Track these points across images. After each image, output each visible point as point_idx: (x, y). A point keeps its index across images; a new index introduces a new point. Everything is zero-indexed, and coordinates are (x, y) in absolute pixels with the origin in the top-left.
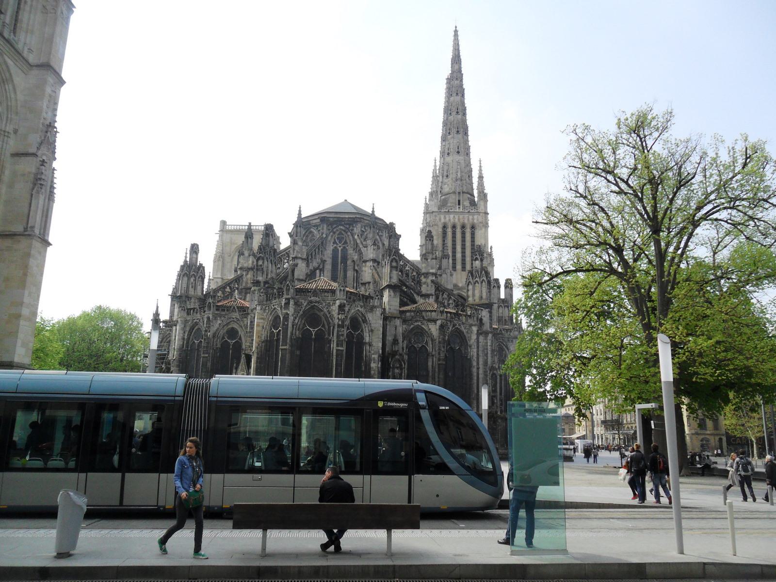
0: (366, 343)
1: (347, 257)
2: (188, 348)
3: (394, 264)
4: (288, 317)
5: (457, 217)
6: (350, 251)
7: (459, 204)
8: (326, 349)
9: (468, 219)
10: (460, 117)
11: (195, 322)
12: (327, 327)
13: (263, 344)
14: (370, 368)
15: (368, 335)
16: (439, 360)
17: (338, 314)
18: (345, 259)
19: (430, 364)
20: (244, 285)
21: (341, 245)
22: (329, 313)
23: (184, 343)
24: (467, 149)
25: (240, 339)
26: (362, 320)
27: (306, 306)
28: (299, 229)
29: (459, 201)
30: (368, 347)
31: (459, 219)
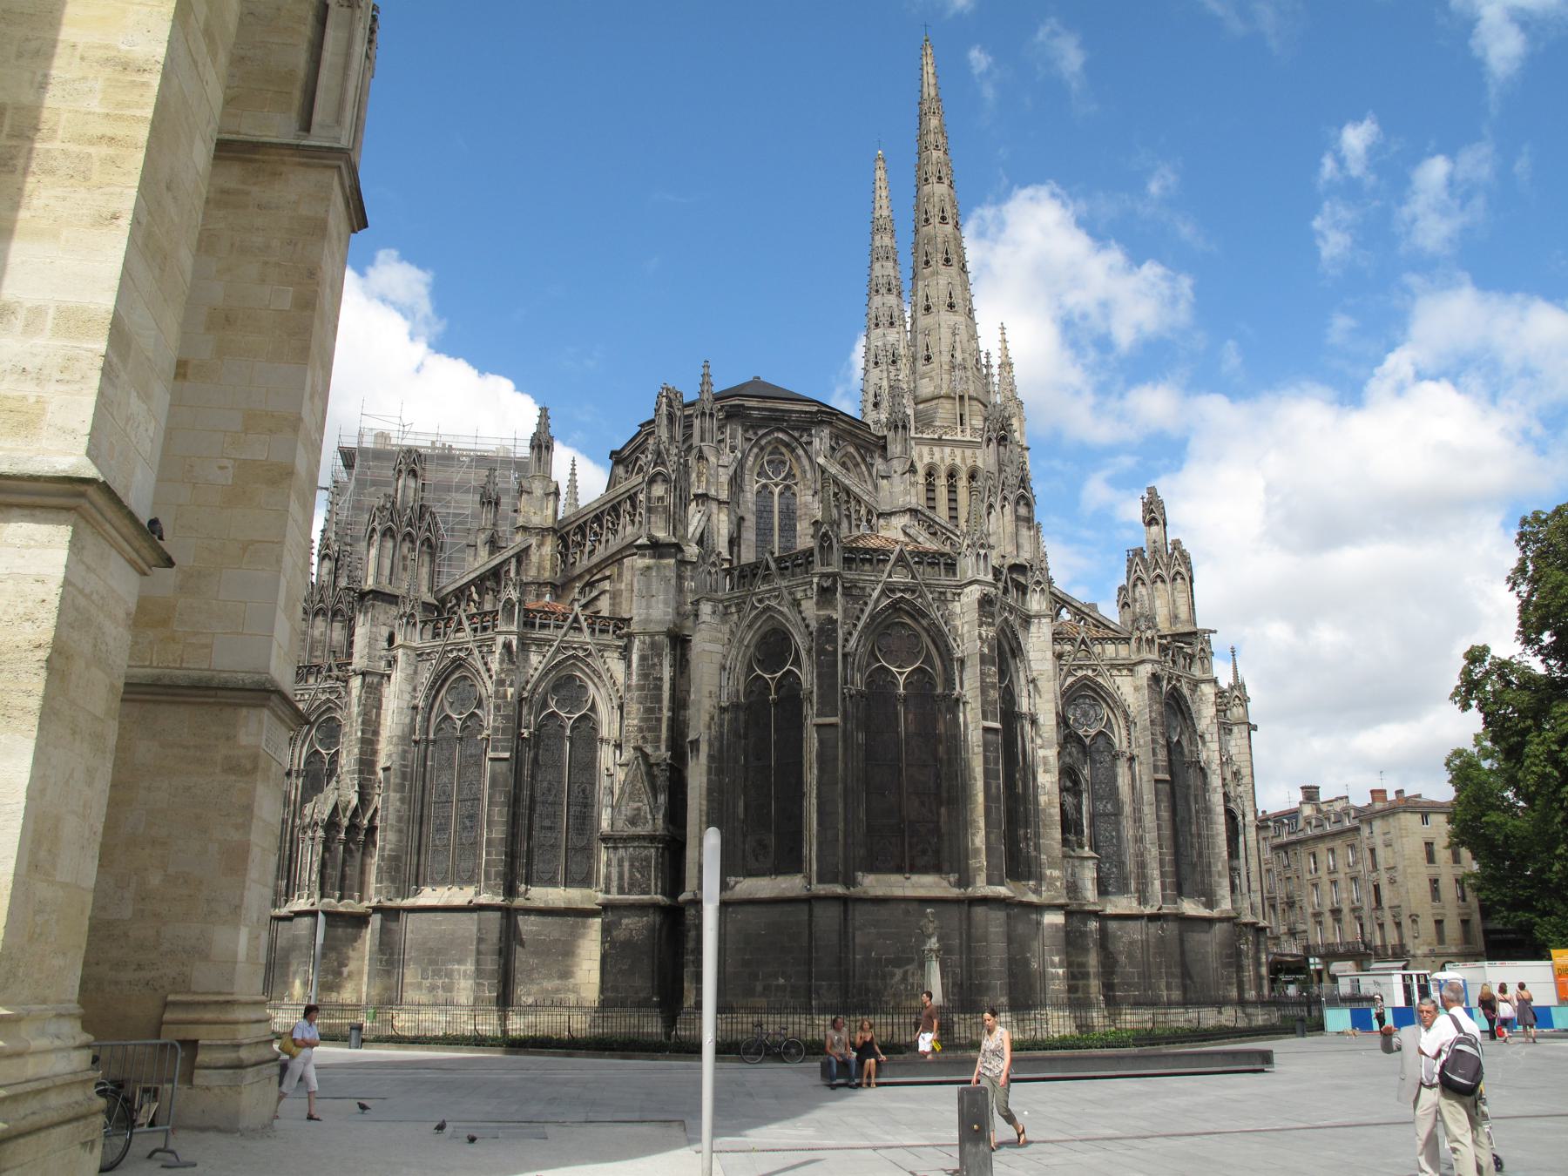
0: (1020, 716)
2: (427, 734)
3: (1023, 511)
4: (835, 631)
8: (941, 728)
10: (949, 228)
11: (454, 660)
12: (938, 662)
13: (726, 717)
14: (1036, 787)
15: (1025, 693)
16: (1156, 769)
17: (980, 626)
19: (1123, 781)
20: (533, 572)
21: (777, 480)
23: (413, 720)
25: (593, 708)
26: (1012, 650)
27: (878, 599)
29: (961, 416)
30: (1028, 727)
31: (963, 459)
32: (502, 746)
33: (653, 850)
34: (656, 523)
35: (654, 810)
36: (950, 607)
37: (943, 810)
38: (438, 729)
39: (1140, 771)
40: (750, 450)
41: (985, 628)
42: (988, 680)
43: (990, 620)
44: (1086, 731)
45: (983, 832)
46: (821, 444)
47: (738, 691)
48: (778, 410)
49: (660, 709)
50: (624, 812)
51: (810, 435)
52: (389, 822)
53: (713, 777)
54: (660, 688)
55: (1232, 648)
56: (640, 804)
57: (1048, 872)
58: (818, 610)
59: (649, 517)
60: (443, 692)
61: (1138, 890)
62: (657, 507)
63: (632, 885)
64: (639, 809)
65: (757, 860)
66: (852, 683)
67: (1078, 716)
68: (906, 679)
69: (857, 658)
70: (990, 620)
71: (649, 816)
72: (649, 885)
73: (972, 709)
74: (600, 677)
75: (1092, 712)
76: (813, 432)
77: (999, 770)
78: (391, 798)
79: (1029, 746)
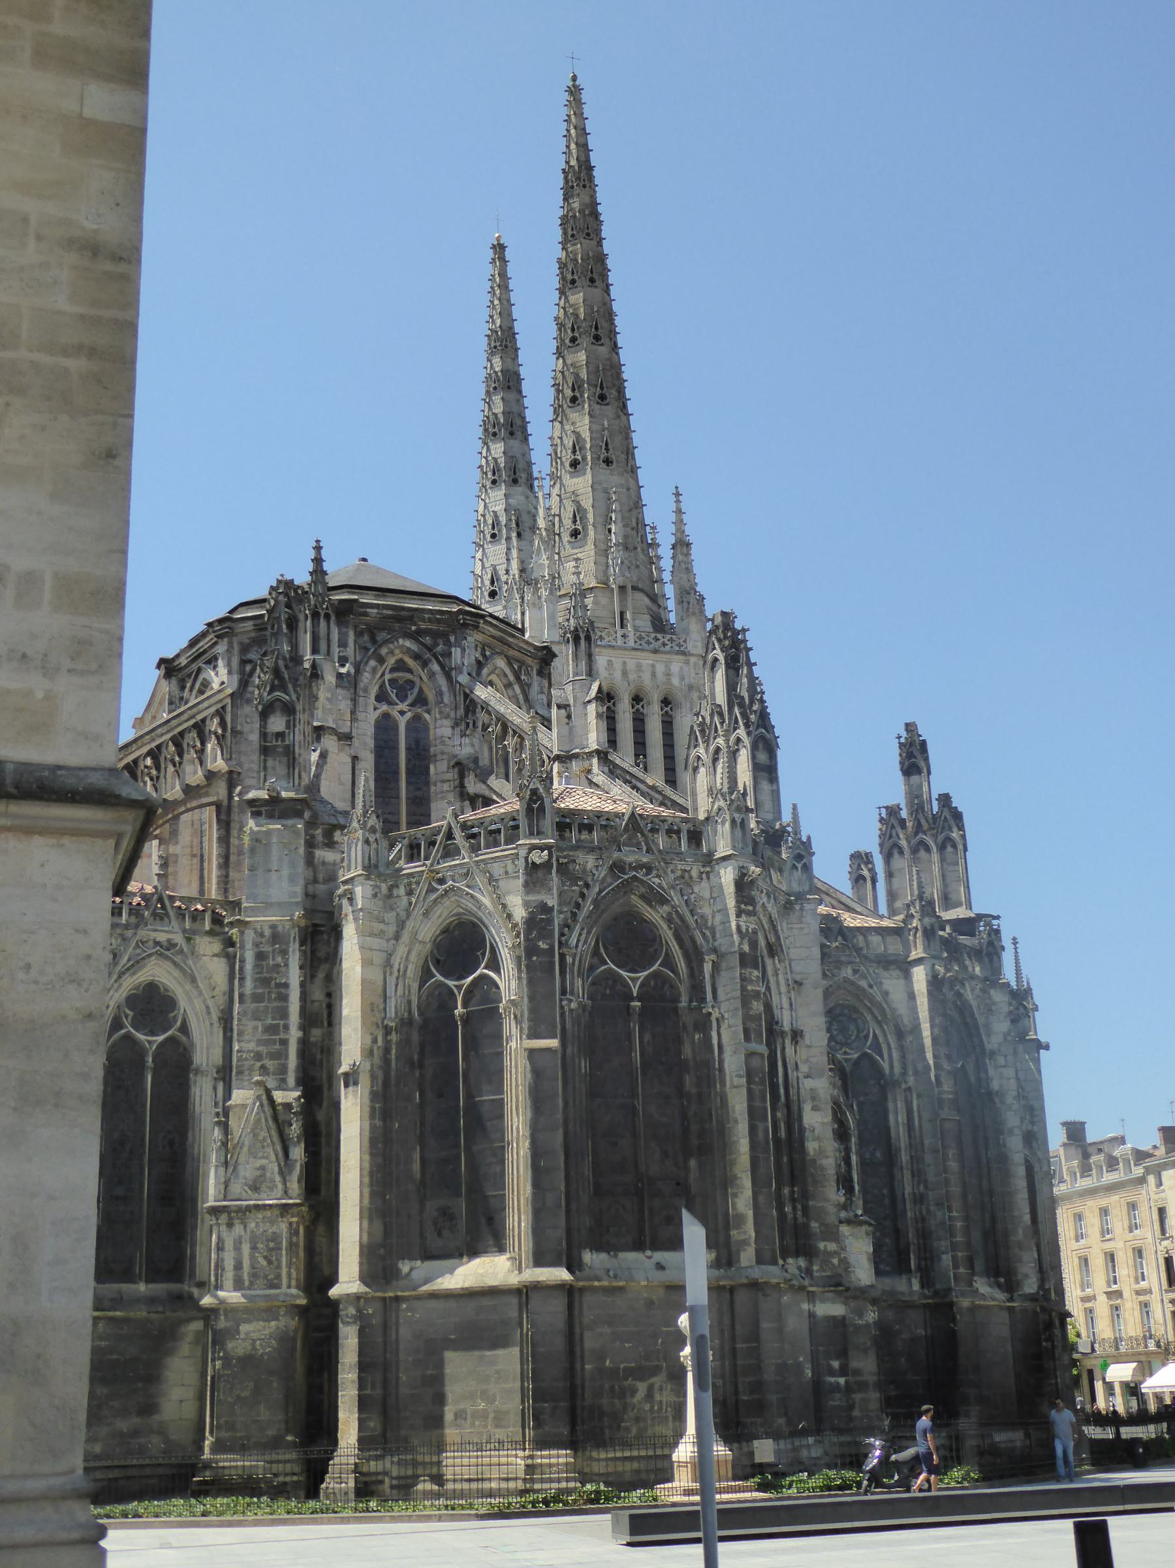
1: (427, 750)
3: (762, 757)
4: (550, 921)
5: (618, 665)
6: (441, 730)
7: (622, 626)
8: (687, 1051)
9: (654, 674)
10: (603, 351)
12: (681, 965)
13: (394, 1037)
14: (802, 1130)
15: (786, 1004)
18: (420, 755)
22: (692, 912)
24: (629, 452)
25: (184, 1029)
26: (769, 946)
28: (323, 623)
29: (622, 614)
31: (625, 673)
34: (274, 768)
35: (285, 1170)
36: (696, 889)
37: (693, 1163)
39: (918, 1106)
40: (367, 663)
41: (744, 917)
42: (749, 988)
43: (751, 908)
44: (846, 1053)
45: (749, 1193)
46: (463, 657)
47: (409, 1002)
48: (403, 609)
49: (286, 1027)
51: (448, 644)
53: (378, 1123)
54: (284, 998)
55: (1014, 939)
56: (264, 1162)
57: (821, 1245)
58: (527, 893)
59: (265, 761)
61: (919, 1268)
62: (276, 746)
63: (254, 1276)
64: (263, 1168)
65: (439, 1234)
66: (572, 993)
67: (835, 1033)
68: (642, 986)
69: (577, 959)
70: (751, 908)
71: (278, 1178)
72: (279, 1276)
73: (729, 1026)
75: (852, 1027)
76: (452, 639)
77: (766, 1109)
79: (792, 1075)
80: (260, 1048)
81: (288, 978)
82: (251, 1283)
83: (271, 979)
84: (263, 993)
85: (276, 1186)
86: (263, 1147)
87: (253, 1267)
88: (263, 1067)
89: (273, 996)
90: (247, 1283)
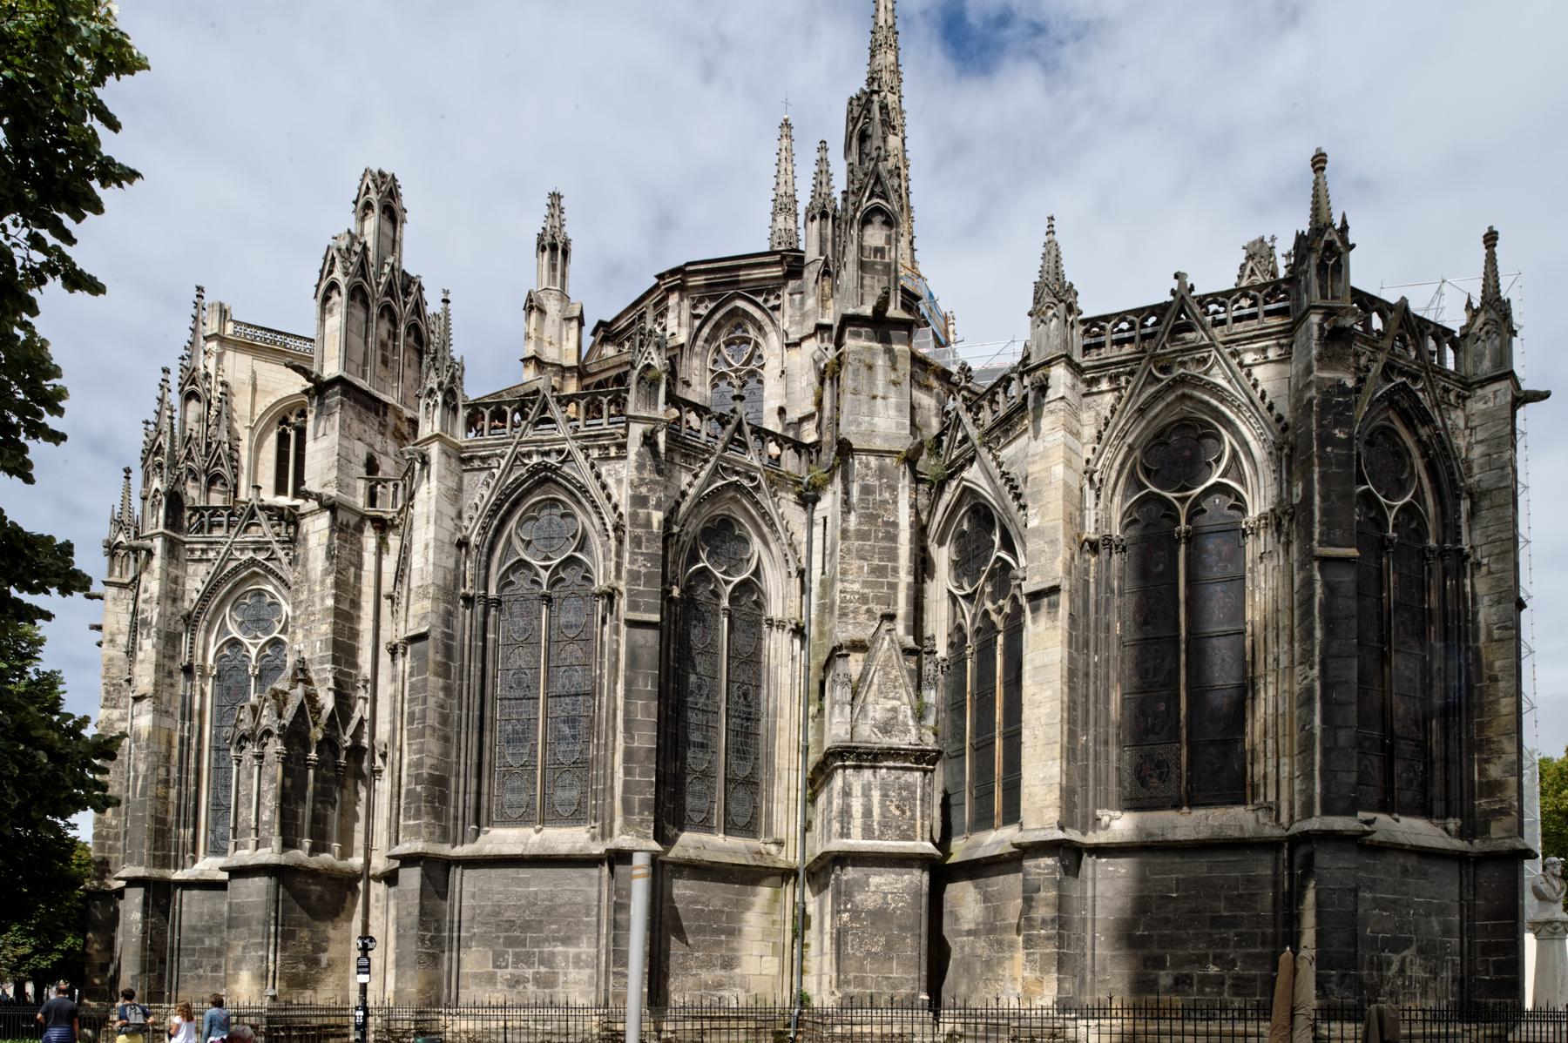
2: (486, 589)
32: (646, 604)
33: (918, 774)
38: (505, 583)
49: (895, 570)
50: (871, 714)
52: (429, 722)
54: (894, 538)
56: (896, 703)
60: (513, 523)
63: (885, 825)
64: (894, 710)
71: (911, 722)
74: (772, 525)
78: (431, 684)
80: (866, 591)
81: (897, 516)
82: (882, 833)
83: (878, 516)
84: (870, 530)
85: (909, 731)
86: (895, 687)
87: (883, 815)
88: (869, 611)
89: (880, 535)
90: (877, 833)
